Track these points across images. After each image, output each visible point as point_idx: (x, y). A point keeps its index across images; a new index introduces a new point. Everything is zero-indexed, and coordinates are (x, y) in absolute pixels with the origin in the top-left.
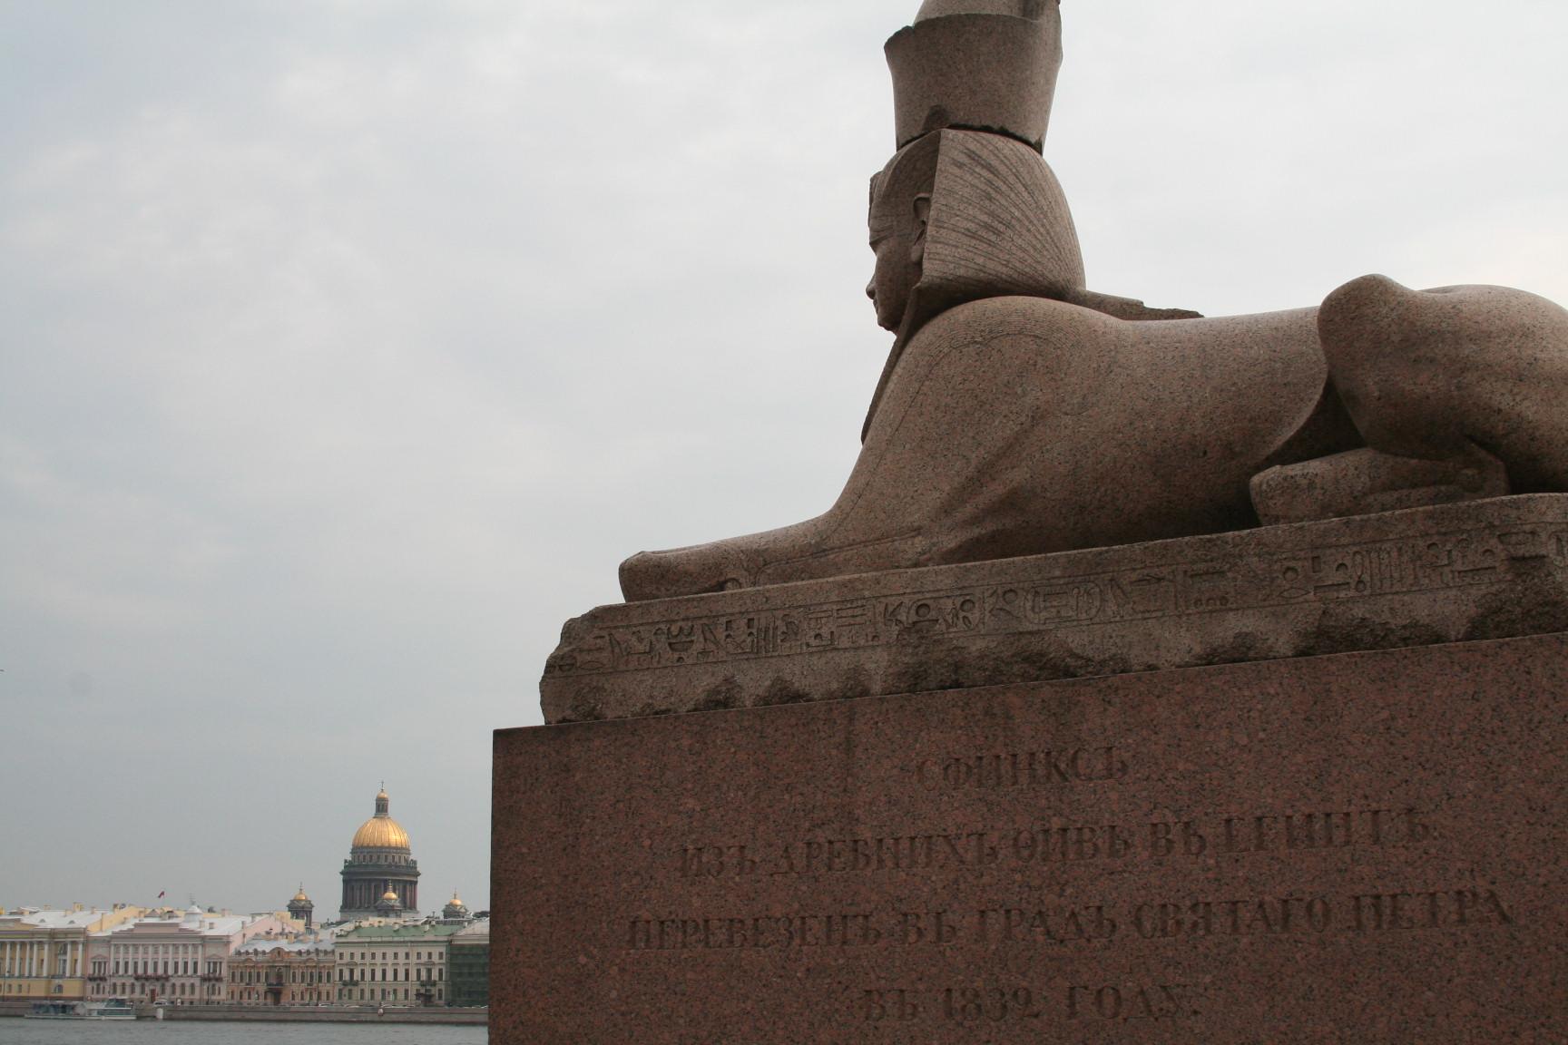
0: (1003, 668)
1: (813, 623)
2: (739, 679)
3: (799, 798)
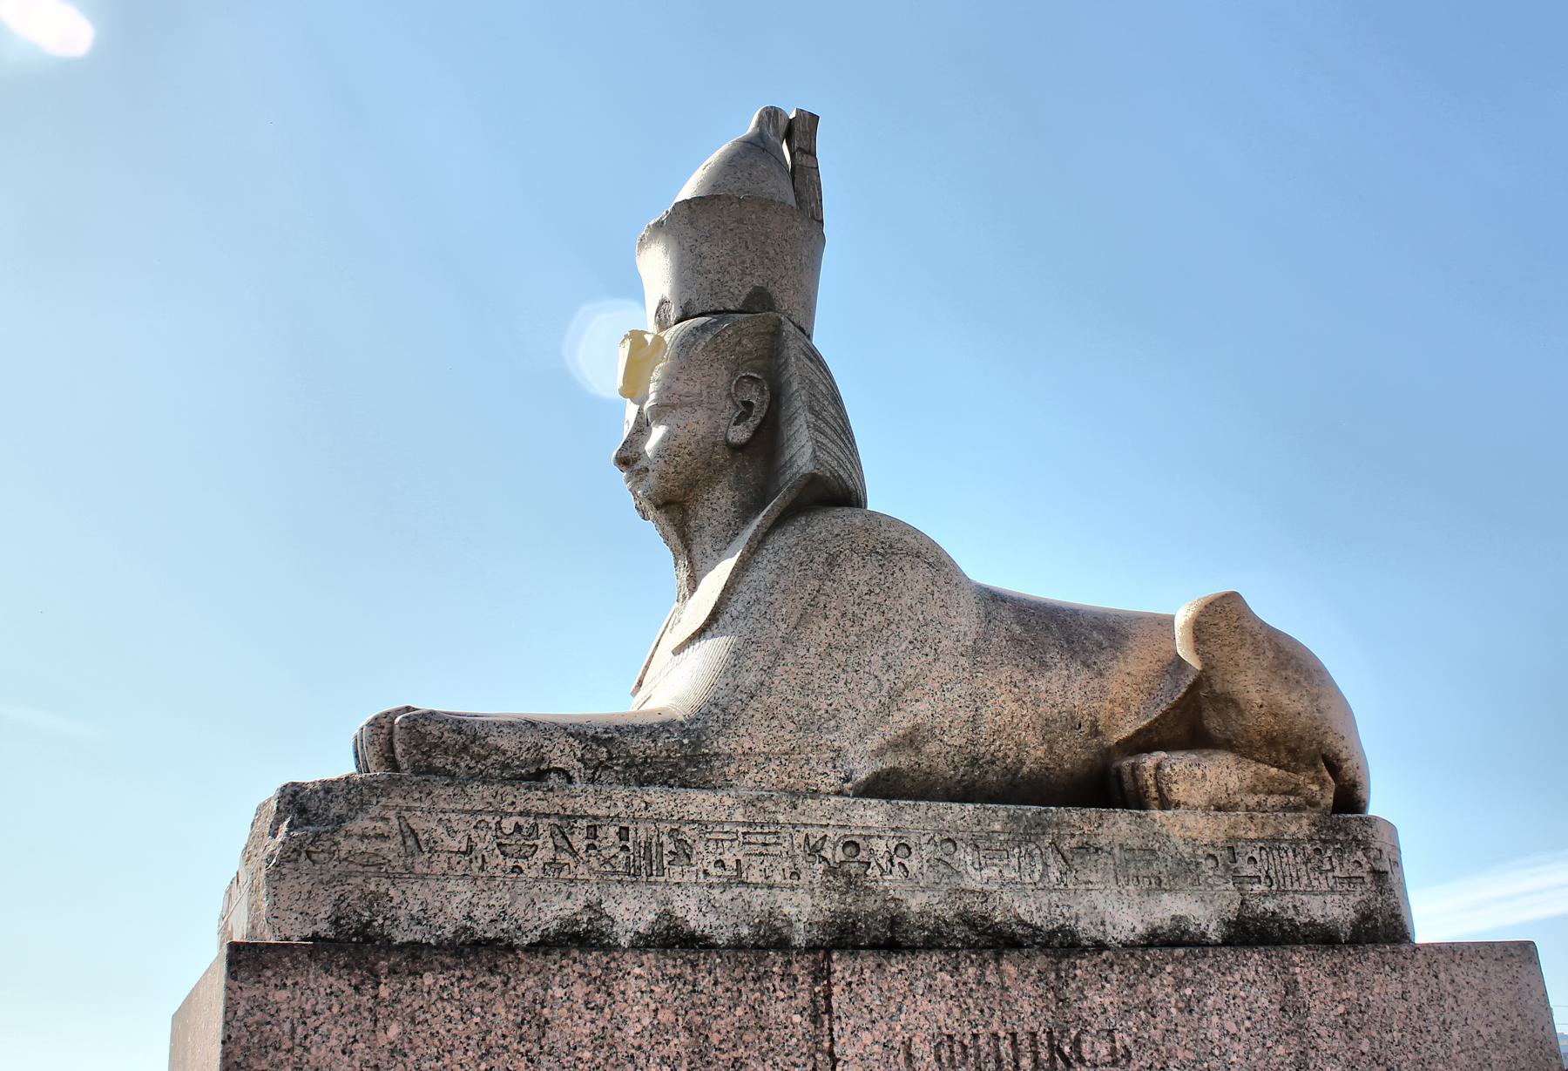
0: (944, 929)
1: (712, 845)
2: (609, 907)
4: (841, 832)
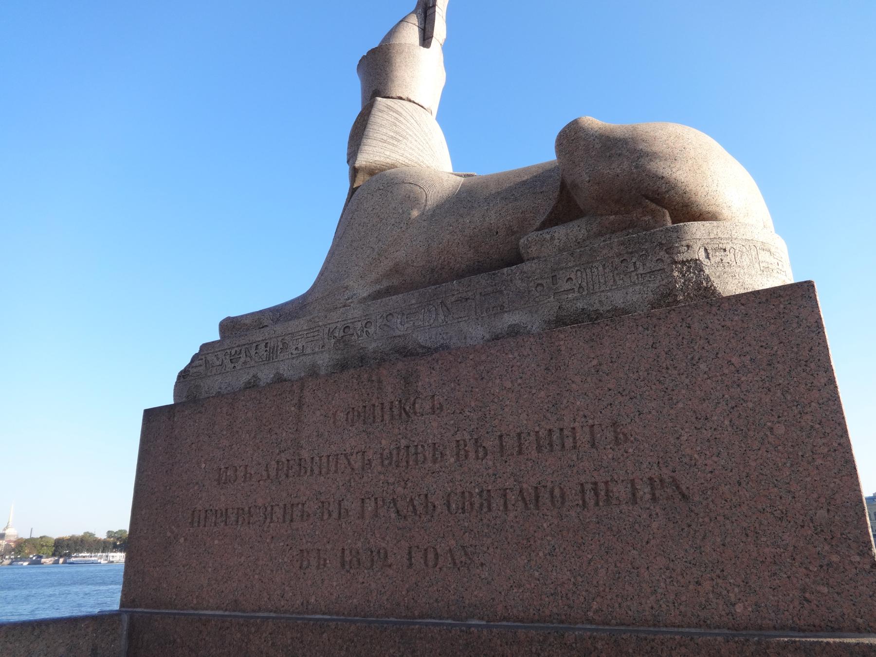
0: (386, 357)
2: (260, 375)
3: (274, 437)
4: (343, 323)
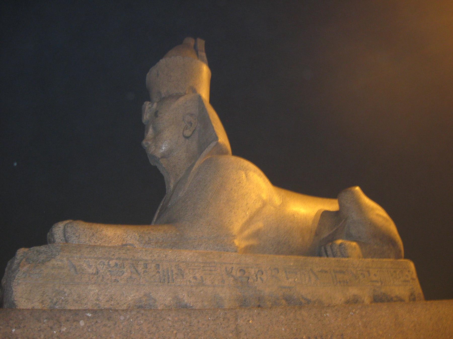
1: (191, 272)
